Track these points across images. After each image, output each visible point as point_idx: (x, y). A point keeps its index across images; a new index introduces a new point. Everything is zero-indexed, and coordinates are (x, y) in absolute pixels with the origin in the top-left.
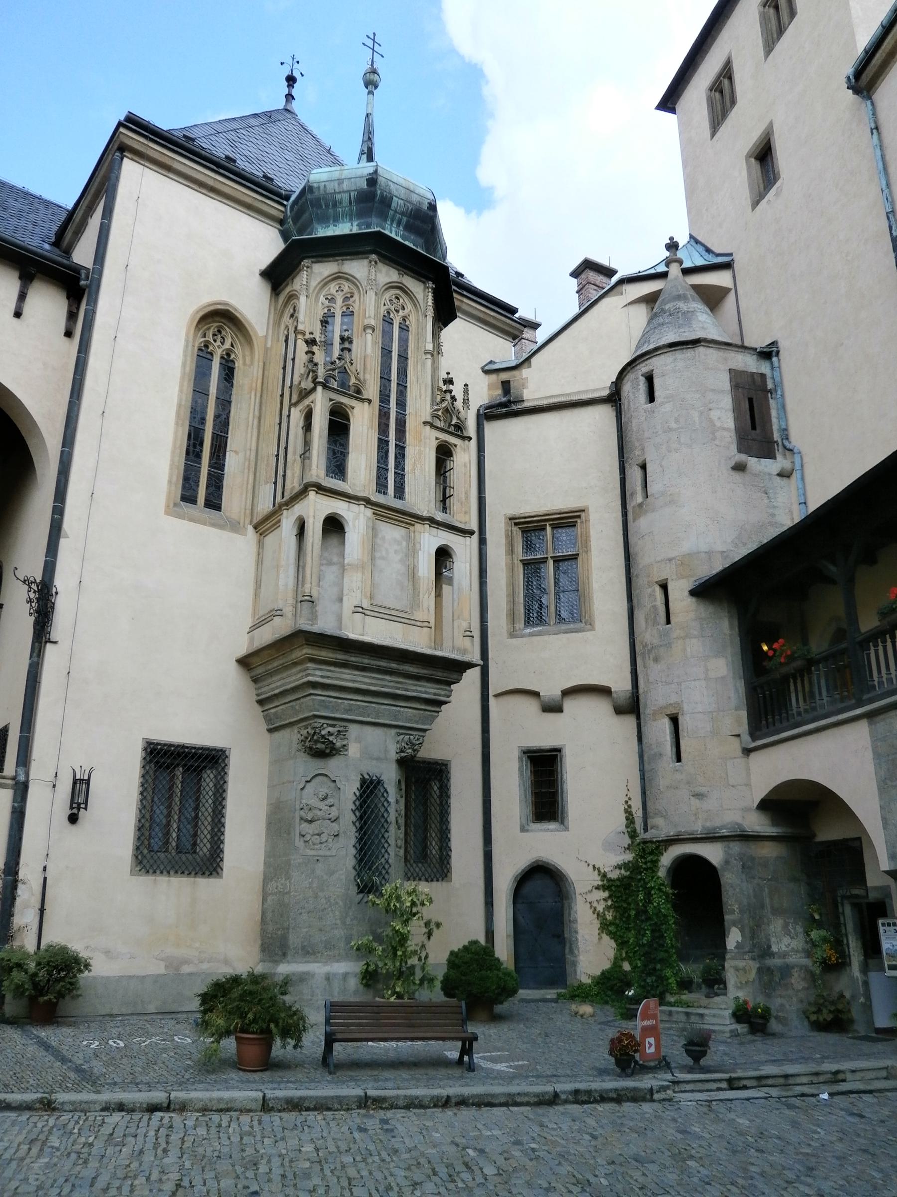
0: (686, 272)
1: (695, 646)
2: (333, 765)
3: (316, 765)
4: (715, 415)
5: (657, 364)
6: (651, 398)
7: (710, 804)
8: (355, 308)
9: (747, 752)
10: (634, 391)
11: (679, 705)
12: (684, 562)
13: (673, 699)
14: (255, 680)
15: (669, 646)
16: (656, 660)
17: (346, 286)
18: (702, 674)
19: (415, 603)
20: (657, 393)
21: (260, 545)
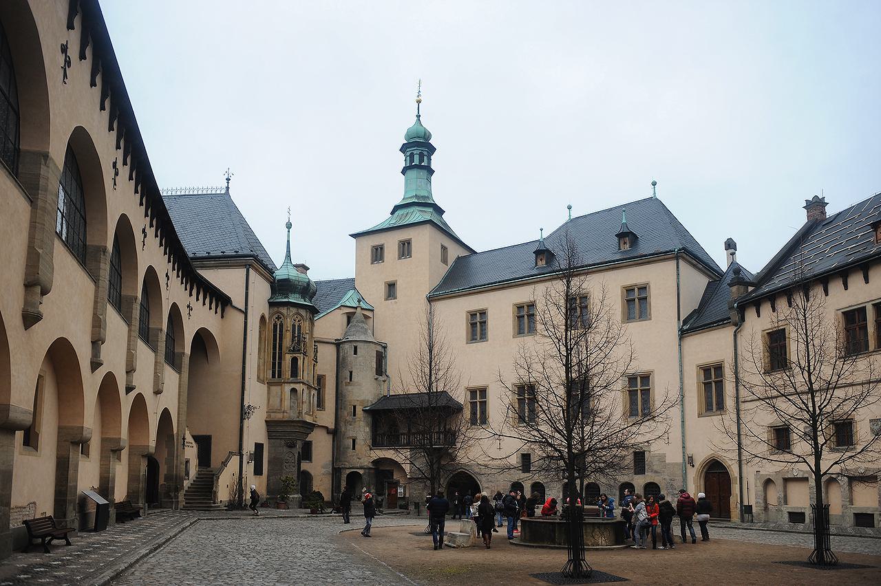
0: (362, 309)
1: (362, 423)
2: (294, 450)
3: (289, 450)
4: (373, 363)
5: (358, 344)
6: (355, 353)
7: (362, 461)
8: (302, 325)
9: (371, 449)
10: (348, 348)
11: (356, 437)
12: (362, 402)
13: (355, 435)
14: (267, 426)
15: (355, 422)
16: (350, 425)
17: (299, 317)
18: (361, 431)
19: (310, 410)
20: (358, 353)
21: (269, 388)
